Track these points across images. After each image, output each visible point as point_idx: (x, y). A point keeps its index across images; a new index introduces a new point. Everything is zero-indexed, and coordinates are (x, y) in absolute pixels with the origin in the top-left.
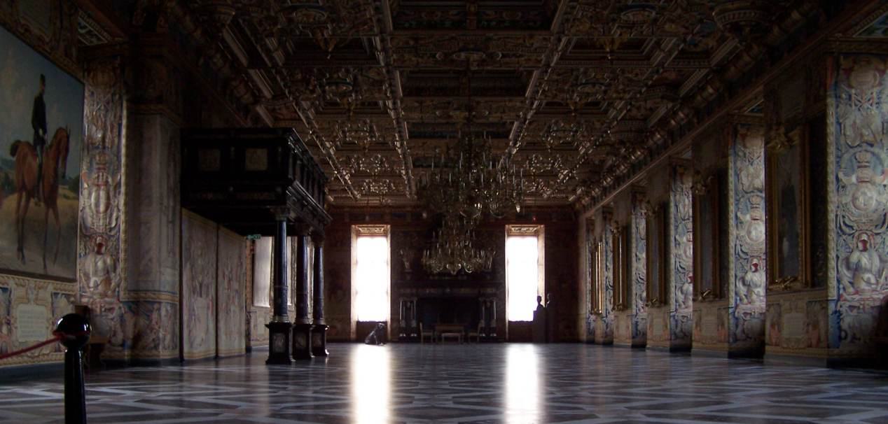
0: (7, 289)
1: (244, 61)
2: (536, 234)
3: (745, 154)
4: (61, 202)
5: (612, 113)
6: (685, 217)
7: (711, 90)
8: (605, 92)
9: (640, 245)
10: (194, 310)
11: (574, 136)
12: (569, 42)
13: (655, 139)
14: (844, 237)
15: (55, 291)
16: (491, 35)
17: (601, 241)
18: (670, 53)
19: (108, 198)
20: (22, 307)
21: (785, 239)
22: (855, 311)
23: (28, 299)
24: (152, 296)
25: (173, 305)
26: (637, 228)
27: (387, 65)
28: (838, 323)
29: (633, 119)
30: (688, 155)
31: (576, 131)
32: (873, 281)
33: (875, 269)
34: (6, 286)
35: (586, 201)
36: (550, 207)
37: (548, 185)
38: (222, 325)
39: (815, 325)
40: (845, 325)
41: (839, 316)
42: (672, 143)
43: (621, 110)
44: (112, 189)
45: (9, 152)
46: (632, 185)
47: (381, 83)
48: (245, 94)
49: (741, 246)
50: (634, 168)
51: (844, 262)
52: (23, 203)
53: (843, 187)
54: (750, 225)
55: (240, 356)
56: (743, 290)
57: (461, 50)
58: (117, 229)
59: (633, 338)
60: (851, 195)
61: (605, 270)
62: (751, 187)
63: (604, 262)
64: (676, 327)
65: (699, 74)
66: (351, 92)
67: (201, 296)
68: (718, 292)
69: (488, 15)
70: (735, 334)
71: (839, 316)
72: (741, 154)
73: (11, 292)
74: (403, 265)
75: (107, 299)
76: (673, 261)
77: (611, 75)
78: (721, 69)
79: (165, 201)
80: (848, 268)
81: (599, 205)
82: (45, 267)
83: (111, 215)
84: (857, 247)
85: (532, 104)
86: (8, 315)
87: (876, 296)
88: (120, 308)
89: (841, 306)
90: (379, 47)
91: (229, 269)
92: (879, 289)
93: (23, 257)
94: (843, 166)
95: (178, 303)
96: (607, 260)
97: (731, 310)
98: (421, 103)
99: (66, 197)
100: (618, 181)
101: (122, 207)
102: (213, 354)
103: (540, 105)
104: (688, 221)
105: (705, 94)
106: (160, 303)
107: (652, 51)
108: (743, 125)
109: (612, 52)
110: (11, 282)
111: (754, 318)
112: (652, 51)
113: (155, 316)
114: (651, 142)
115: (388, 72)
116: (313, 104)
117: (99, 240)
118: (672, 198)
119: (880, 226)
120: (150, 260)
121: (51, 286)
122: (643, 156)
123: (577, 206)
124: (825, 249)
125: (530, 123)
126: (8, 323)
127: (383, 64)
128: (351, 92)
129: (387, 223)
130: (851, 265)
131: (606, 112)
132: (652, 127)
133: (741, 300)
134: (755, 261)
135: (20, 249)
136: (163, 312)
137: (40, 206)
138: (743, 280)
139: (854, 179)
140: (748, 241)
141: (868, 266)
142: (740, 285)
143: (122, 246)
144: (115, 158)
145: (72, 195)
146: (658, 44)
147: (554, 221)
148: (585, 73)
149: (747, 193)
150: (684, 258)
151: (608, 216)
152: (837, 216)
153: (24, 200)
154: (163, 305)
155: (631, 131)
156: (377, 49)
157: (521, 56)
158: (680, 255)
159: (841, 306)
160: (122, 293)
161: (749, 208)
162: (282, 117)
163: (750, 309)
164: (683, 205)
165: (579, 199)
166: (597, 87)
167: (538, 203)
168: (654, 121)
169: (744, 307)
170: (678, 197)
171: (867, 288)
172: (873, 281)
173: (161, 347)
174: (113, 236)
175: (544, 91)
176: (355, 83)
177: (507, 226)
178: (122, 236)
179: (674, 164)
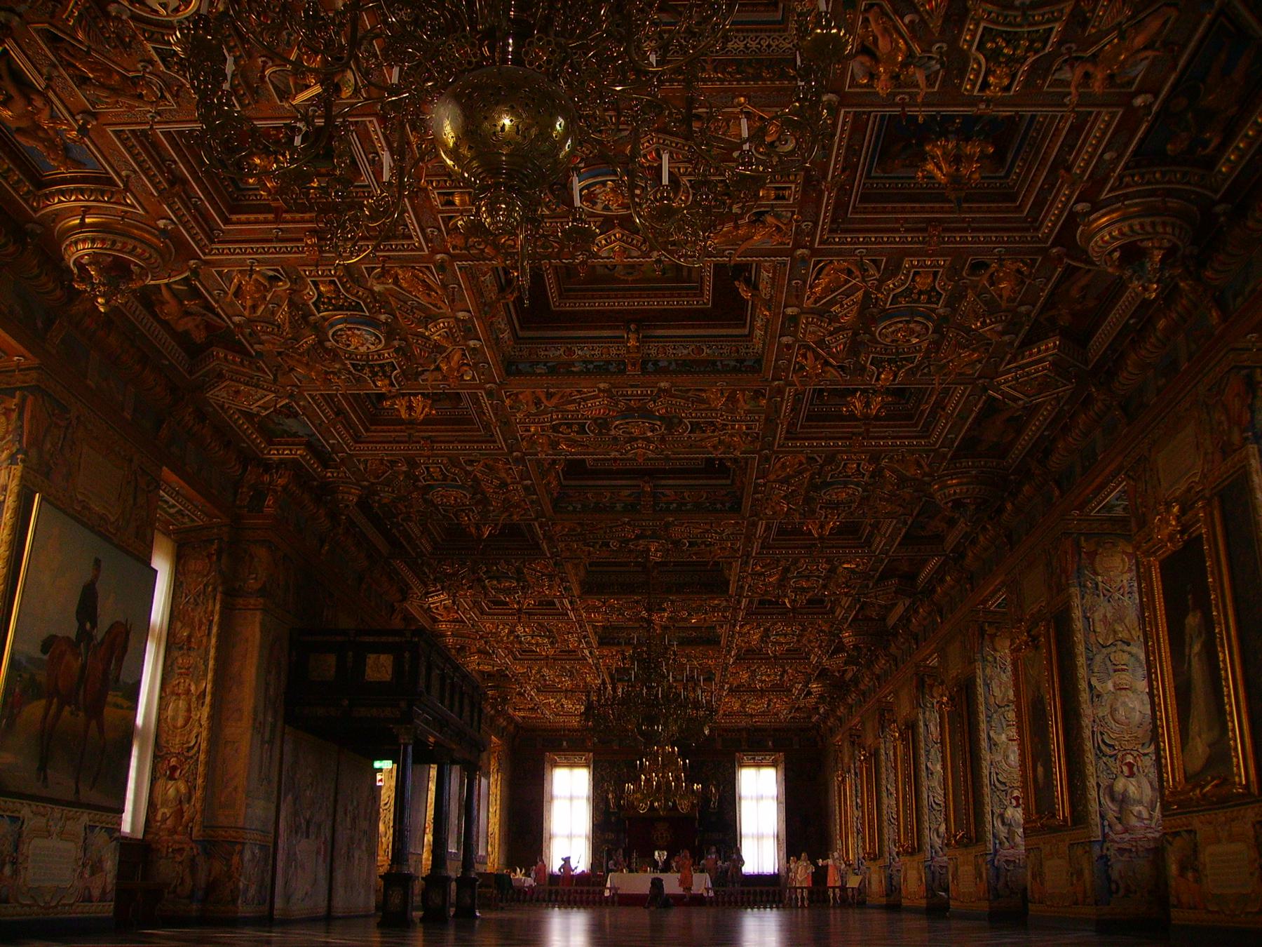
0: (18, 818)
2: (774, 764)
3: (995, 658)
4: (110, 714)
5: (840, 613)
8: (825, 587)
10: (295, 854)
11: (798, 641)
12: (768, 528)
14: (1104, 759)
15: (91, 824)
17: (849, 771)
19: (189, 710)
20: (38, 842)
21: (1039, 764)
22: (1126, 854)
23: (49, 832)
24: (234, 834)
25: (263, 848)
28: (1106, 871)
30: (934, 662)
31: (801, 636)
32: (1145, 815)
33: (1146, 799)
34: (16, 814)
38: (339, 875)
39: (1080, 874)
40: (1115, 875)
41: (1106, 864)
44: (194, 699)
45: (39, 648)
46: (879, 701)
49: (997, 774)
51: (1107, 791)
52: (52, 712)
53: (1098, 696)
54: (1007, 748)
55: (367, 916)
56: (1002, 831)
57: (638, 537)
58: (196, 749)
59: (887, 895)
60: (1108, 706)
64: (933, 880)
67: (308, 837)
68: (973, 834)
69: (665, 495)
70: (996, 889)
71: (1106, 864)
73: (23, 823)
74: (607, 801)
75: (176, 837)
77: (828, 567)
79: (261, 717)
80: (1113, 799)
82: (77, 792)
83: (191, 731)
84: (1122, 772)
85: (739, 602)
86: (16, 851)
87: (1150, 835)
88: (192, 848)
89: (1108, 849)
91: (355, 803)
92: (1153, 825)
93: (45, 778)
94: (1096, 670)
95: (271, 845)
97: (989, 858)
99: (117, 706)
101: (204, 722)
102: (322, 911)
103: (751, 602)
106: (243, 844)
107: (871, 534)
110: (26, 811)
111: (1020, 867)
112: (871, 534)
113: (236, 858)
115: (555, 564)
117: (173, 761)
118: (921, 716)
119: (1147, 745)
120: (236, 789)
121: (85, 818)
124: (1083, 778)
126: (14, 863)
129: (589, 751)
130: (1116, 796)
131: (832, 611)
133: (1000, 843)
134: (1016, 793)
135: (42, 768)
136: (247, 855)
137: (78, 715)
138: (1002, 816)
139: (1110, 685)
140: (1005, 767)
141: (1137, 797)
142: (998, 824)
143: (201, 769)
144: (202, 662)
145: (126, 703)
152: (1093, 732)
153: (54, 707)
154: (247, 846)
159: (1108, 849)
160: (195, 831)
162: (440, 618)
163: (1013, 855)
164: (931, 725)
168: (892, 619)
169: (1006, 852)
171: (1138, 824)
172: (1145, 815)
173: (240, 901)
174: (191, 757)
175: (750, 586)
178: (202, 757)
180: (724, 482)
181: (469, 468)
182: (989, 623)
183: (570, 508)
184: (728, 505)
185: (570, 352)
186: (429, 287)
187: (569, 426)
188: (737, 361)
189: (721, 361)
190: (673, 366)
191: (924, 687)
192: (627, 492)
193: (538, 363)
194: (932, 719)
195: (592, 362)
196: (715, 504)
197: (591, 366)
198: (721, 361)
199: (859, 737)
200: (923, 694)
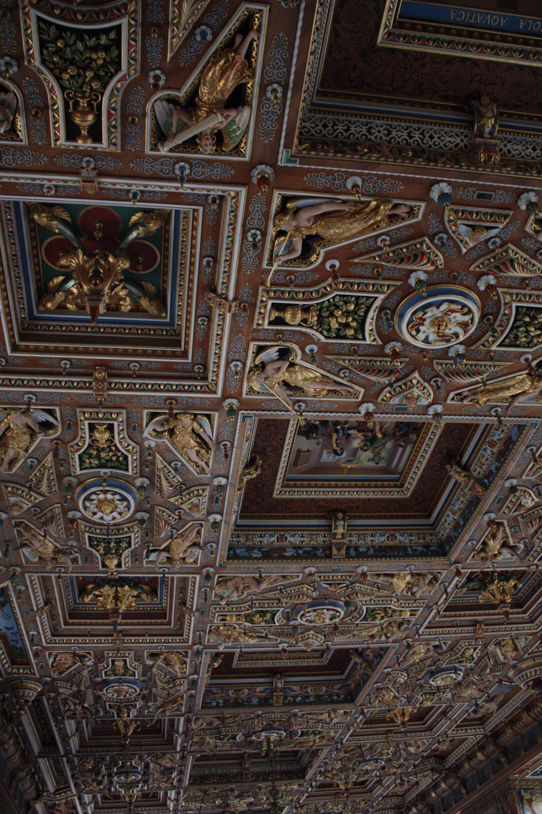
1: (36, 748)
16: (297, 710)
27: (183, 749)
47: (170, 770)
48: (28, 789)
66: (138, 782)
78: (496, 734)
90: (181, 730)
98: (205, 792)
105: (474, 762)
108: (526, 790)
109: (403, 723)
116: (94, 797)
127: (178, 749)
128: (138, 782)
148: (371, 748)
155: (391, 808)
156: (177, 732)
176: (146, 773)
180: (338, 677)
181: (149, 662)
182: (524, 789)
183: (214, 704)
184: (342, 697)
185: (281, 538)
186: (203, 443)
187: (263, 614)
188: (424, 546)
189: (411, 547)
190: (371, 552)
193: (253, 548)
195: (300, 548)
196: (332, 696)
197: (301, 552)
198: (411, 547)
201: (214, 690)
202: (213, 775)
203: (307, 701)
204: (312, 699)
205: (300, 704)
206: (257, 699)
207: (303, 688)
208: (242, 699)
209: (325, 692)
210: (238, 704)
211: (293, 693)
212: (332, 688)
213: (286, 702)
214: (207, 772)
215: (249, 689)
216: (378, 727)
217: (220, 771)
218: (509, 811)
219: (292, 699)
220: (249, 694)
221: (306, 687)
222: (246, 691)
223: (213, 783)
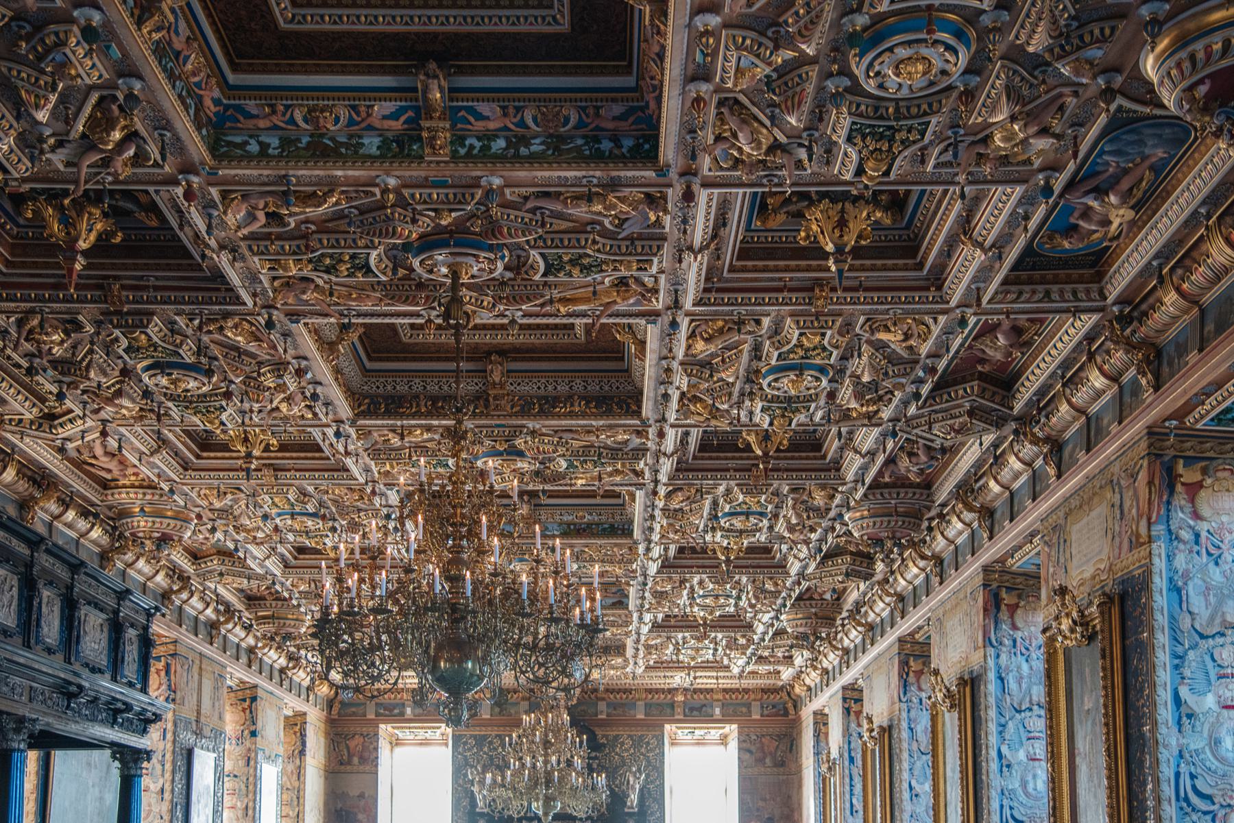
2: (724, 740)
6: (1020, 704)
7: (1097, 381)
9: (919, 764)
13: (950, 533)
18: (999, 247)
26: (911, 729)
29: (901, 483)
35: (812, 678)
36: (746, 691)
37: (732, 645)
42: (991, 538)
43: (872, 454)
46: (901, 640)
50: (903, 603)
54: (1218, 723)
61: (848, 812)
62: (1218, 621)
63: (848, 796)
65: (1073, 330)
69: (480, 117)
72: (1185, 535)
76: (995, 805)
81: (836, 686)
85: (661, 435)
96: (852, 794)
100: (872, 631)
103: (684, 442)
104: (1028, 714)
114: (940, 544)
122: (923, 576)
123: (797, 690)
125: (669, 495)
131: (836, 466)
132: (943, 505)
146: (965, 225)
147: (756, 716)
149: (1202, 636)
150: (1023, 798)
151: (855, 707)
157: (599, 267)
158: (1013, 791)
161: (1213, 677)
165: (798, 676)
166: (808, 379)
167: (725, 683)
170: (1004, 657)
175: (683, 394)
177: (667, 727)
179: (995, 585)
184: (628, 143)
191: (998, 608)
192: (389, 107)
194: (1012, 667)
196: (597, 140)
199: (856, 701)
200: (997, 623)
201: (251, 105)
202: (417, 397)
203: (523, 151)
204: (536, 146)
205: (500, 158)
206: (376, 141)
207: (511, 111)
208: (332, 139)
209: (575, 128)
210: (322, 151)
211: (480, 125)
212: (597, 115)
213: (462, 151)
214: (402, 388)
215: (354, 108)
216: (787, 269)
217: (433, 388)
218: (1134, 511)
219: (478, 144)
220: (351, 122)
221: (518, 109)
222: (344, 114)
223: (417, 415)
